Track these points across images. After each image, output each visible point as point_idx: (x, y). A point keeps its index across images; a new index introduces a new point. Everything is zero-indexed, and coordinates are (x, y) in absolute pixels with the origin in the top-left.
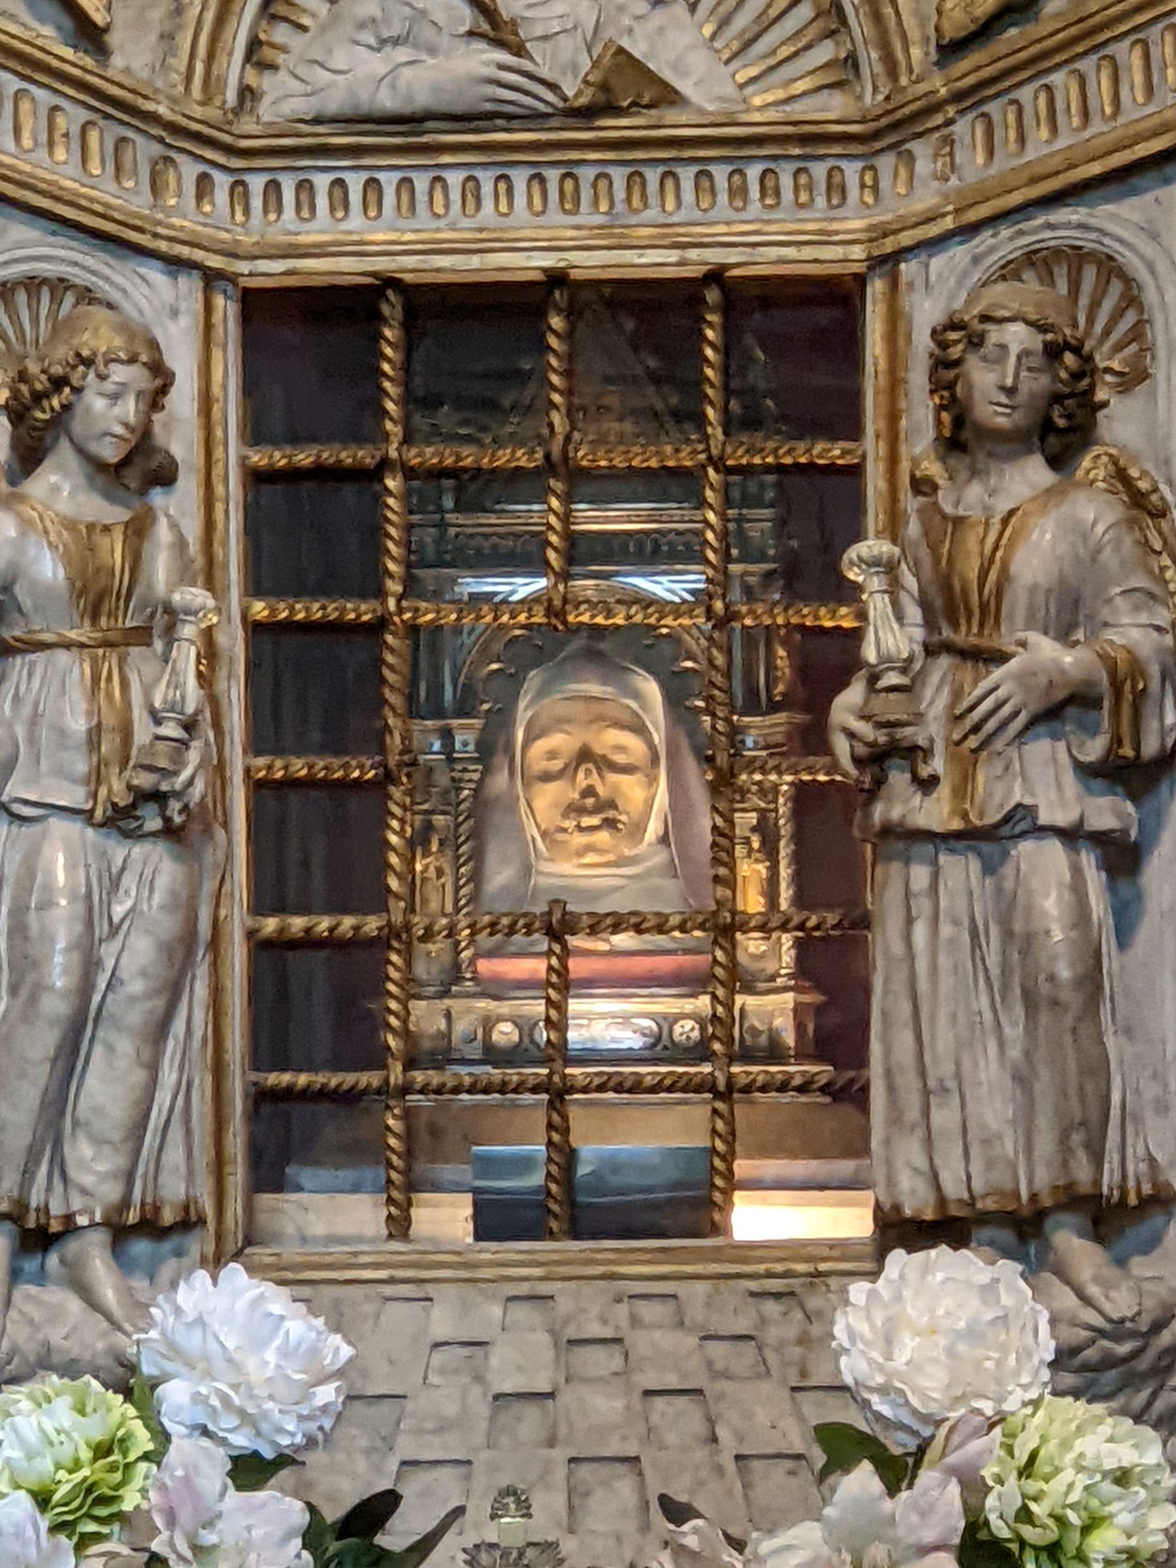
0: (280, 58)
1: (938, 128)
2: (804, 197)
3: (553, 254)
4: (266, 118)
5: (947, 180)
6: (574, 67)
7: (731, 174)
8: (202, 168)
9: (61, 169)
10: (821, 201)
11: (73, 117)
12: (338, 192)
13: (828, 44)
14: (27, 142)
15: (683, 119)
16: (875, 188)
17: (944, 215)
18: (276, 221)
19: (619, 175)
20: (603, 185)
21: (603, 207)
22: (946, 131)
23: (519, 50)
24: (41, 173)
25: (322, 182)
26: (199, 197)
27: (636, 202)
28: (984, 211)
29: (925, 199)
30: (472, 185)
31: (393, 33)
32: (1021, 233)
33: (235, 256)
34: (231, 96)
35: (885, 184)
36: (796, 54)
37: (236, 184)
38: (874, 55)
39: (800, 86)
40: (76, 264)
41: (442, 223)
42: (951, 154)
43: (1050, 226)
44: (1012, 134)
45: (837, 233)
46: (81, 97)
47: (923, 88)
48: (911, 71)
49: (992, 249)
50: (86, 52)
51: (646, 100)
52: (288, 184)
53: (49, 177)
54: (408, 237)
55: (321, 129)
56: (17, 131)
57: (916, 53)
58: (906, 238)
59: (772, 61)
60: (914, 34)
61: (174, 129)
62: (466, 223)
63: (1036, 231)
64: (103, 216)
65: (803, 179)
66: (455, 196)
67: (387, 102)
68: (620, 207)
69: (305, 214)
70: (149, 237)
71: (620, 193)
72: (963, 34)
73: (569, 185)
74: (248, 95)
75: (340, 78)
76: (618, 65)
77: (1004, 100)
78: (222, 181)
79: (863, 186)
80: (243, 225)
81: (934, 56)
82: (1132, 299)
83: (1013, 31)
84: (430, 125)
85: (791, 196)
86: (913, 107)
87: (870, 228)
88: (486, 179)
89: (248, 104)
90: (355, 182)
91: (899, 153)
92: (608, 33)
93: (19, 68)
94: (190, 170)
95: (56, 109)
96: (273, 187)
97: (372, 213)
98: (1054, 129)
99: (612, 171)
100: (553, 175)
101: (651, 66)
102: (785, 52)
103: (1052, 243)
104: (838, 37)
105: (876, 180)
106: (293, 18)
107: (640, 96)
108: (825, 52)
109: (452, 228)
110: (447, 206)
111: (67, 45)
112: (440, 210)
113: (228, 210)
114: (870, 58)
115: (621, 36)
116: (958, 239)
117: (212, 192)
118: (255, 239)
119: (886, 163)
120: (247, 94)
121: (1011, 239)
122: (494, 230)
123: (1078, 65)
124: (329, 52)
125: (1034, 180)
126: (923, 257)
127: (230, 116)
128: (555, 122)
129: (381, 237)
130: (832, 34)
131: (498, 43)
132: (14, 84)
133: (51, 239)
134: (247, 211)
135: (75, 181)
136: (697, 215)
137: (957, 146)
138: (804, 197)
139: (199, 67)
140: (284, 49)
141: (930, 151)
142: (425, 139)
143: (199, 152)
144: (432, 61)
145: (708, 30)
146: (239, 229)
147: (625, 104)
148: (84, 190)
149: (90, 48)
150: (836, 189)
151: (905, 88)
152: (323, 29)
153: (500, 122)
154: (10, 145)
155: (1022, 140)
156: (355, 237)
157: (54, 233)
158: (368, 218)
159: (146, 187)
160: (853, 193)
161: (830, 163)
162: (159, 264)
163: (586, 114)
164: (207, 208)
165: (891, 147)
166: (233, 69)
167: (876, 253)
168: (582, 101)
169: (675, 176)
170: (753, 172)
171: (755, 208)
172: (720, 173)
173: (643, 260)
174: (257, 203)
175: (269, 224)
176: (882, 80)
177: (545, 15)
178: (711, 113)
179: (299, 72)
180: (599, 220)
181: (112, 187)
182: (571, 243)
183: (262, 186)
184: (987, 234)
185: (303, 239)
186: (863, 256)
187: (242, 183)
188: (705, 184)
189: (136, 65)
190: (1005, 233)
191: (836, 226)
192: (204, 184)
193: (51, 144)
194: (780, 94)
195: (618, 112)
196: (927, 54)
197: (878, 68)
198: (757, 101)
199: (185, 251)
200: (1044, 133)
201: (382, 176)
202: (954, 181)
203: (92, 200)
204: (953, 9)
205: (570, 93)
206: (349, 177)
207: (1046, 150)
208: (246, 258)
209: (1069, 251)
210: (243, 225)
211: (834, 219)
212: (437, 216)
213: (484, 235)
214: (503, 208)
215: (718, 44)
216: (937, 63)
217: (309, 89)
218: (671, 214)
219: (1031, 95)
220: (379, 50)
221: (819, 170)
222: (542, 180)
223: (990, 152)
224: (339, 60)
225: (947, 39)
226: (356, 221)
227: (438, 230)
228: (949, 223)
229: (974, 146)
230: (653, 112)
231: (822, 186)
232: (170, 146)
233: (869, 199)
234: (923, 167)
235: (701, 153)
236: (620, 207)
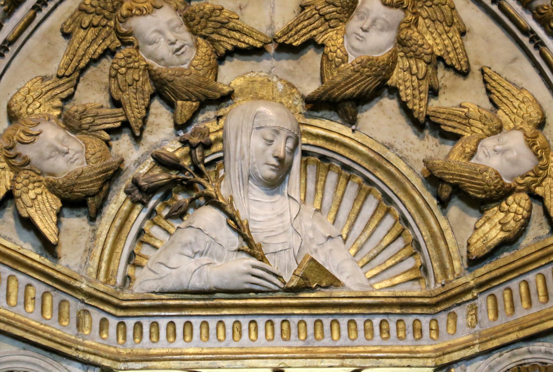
0: (144, 262)
1: (468, 301)
2: (401, 334)
3: (277, 361)
4: (136, 291)
5: (474, 327)
6: (289, 269)
7: (365, 322)
8: (104, 315)
9: (31, 316)
10: (410, 336)
11: (38, 289)
12: (171, 329)
13: (411, 259)
14: (13, 301)
15: (342, 294)
16: (437, 330)
17: (474, 345)
18: (140, 342)
19: (310, 321)
20: (302, 325)
21: (302, 337)
22: (472, 303)
23: (262, 259)
24: (18, 317)
25: (163, 323)
26: (101, 330)
27: (319, 335)
28: (496, 343)
29: (463, 337)
30: (237, 326)
31: (201, 250)
32: (514, 355)
33: (118, 361)
34: (119, 280)
35: (442, 328)
36: (396, 263)
37: (120, 323)
38: (435, 265)
39: (398, 280)
40: (35, 364)
41: (222, 344)
42: (476, 314)
43: (530, 352)
44: (508, 305)
45: (418, 352)
46: (43, 279)
47: (462, 280)
48: (454, 272)
49: (499, 363)
50: (47, 257)
51: (324, 284)
52: (146, 324)
53: (23, 319)
54: (205, 351)
55: (163, 296)
56: (8, 296)
57: (457, 264)
58: (456, 356)
59: (384, 268)
60: (455, 255)
61: (90, 296)
62: (235, 344)
63: (524, 353)
64: (49, 340)
65: (401, 325)
66: (229, 331)
67: (197, 283)
68: (311, 337)
69: (154, 339)
70: (73, 350)
71: (310, 330)
72: (482, 254)
73: (285, 325)
74: (128, 280)
75: (173, 271)
76: (311, 267)
77: (502, 288)
78: (113, 322)
79: (431, 329)
80: (122, 344)
81: (466, 266)
83: (506, 254)
84: (218, 295)
85: (396, 333)
86: (457, 290)
87: (436, 350)
88: (245, 322)
89: (127, 285)
90: (179, 323)
91: (449, 314)
92: (306, 251)
93: (10, 264)
94: (97, 316)
95: (29, 285)
96: (139, 325)
97: (188, 339)
98: (530, 303)
99: (306, 319)
100: (277, 321)
101: (327, 268)
102: (390, 263)
103: (530, 361)
104: (416, 256)
105: (437, 327)
106: (152, 243)
107: (321, 282)
108: (410, 263)
109: (227, 346)
110: (225, 336)
111: (37, 253)
112: (221, 337)
113: (116, 337)
114: (434, 267)
115: (312, 253)
116: (480, 357)
117: (107, 328)
118: (129, 351)
119: (442, 318)
120: (127, 279)
121: (510, 357)
122: (248, 348)
123: (542, 271)
124: (168, 259)
125: (522, 329)
126: (463, 365)
127: (118, 290)
128: (279, 294)
129: (191, 351)
130: (413, 254)
131: (252, 255)
132: (7, 272)
133: (23, 352)
134: (125, 338)
135: (37, 322)
136: (349, 342)
137: (479, 310)
138: (401, 334)
139: (104, 265)
140: (147, 258)
141: (465, 313)
142: (215, 302)
143: (102, 307)
144: (219, 264)
145: (353, 251)
146: (120, 346)
147: (314, 286)
148: (42, 326)
149: (48, 254)
150: (418, 331)
151: (451, 281)
152: (166, 248)
153: (252, 294)
154: (5, 304)
155: (513, 307)
156: (179, 351)
157: (24, 349)
158: (186, 342)
159: (74, 325)
160: (426, 333)
161: (415, 317)
162: (79, 365)
164: (105, 336)
165: (444, 310)
167: (439, 363)
168: (293, 284)
169: (338, 323)
170: (376, 321)
171: (377, 338)
172: (360, 321)
173: (323, 364)
174: (130, 333)
175: (136, 343)
176: (440, 277)
177: (274, 242)
178: (356, 292)
179: (153, 269)
180: (301, 343)
181: (57, 325)
182: (286, 355)
183: (133, 325)
184: (496, 355)
185: (152, 351)
186: (433, 364)
187: (123, 323)
188: (352, 326)
189: (71, 264)
190: (506, 355)
191: (418, 349)
192: (103, 323)
193: (25, 304)
194: (388, 283)
195: (310, 289)
196: (462, 265)
197: (438, 271)
198: (377, 286)
199: (92, 358)
200: (525, 304)
201: (193, 320)
202: (477, 328)
203: (44, 331)
204: (476, 242)
205: (287, 280)
206: (177, 321)
207: (526, 313)
208: (123, 361)
209: (539, 364)
210: (122, 344)
211: (418, 345)
212: (220, 341)
213: (243, 351)
214: (253, 337)
215: (357, 258)
216: (467, 269)
217: (157, 276)
218: (336, 341)
219: (517, 286)
220: (193, 258)
221: (409, 321)
222: (272, 324)
223: (496, 314)
224: (173, 262)
225: (474, 257)
227: (221, 348)
228: (476, 349)
229: (488, 310)
230: (327, 290)
231: (411, 329)
232: (86, 304)
233: (434, 336)
234: (461, 320)
235: (351, 311)
236: (311, 337)
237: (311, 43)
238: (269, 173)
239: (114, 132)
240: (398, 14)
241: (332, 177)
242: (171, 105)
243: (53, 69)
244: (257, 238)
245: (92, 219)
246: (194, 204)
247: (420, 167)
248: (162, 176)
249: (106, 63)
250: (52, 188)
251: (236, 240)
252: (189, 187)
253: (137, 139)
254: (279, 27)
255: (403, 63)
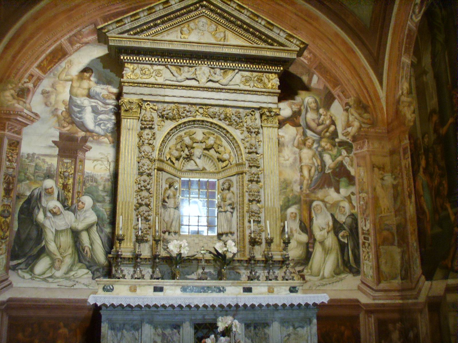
11: (173, 169)
29: (221, 176)
82: (232, 182)
163: (202, 170)
166: (182, 167)
226: (188, 176)
237: (204, 142)
238: (199, 157)
239: (181, 151)
240: (214, 139)
241: (206, 158)
242: (188, 148)
243: (174, 143)
244: (198, 164)
245: (178, 161)
246: (190, 160)
247: (217, 157)
248: (186, 156)
249: (180, 143)
250: (175, 157)
251: (195, 164)
252: (189, 158)
253: (184, 152)
254: (201, 140)
255: (215, 145)
